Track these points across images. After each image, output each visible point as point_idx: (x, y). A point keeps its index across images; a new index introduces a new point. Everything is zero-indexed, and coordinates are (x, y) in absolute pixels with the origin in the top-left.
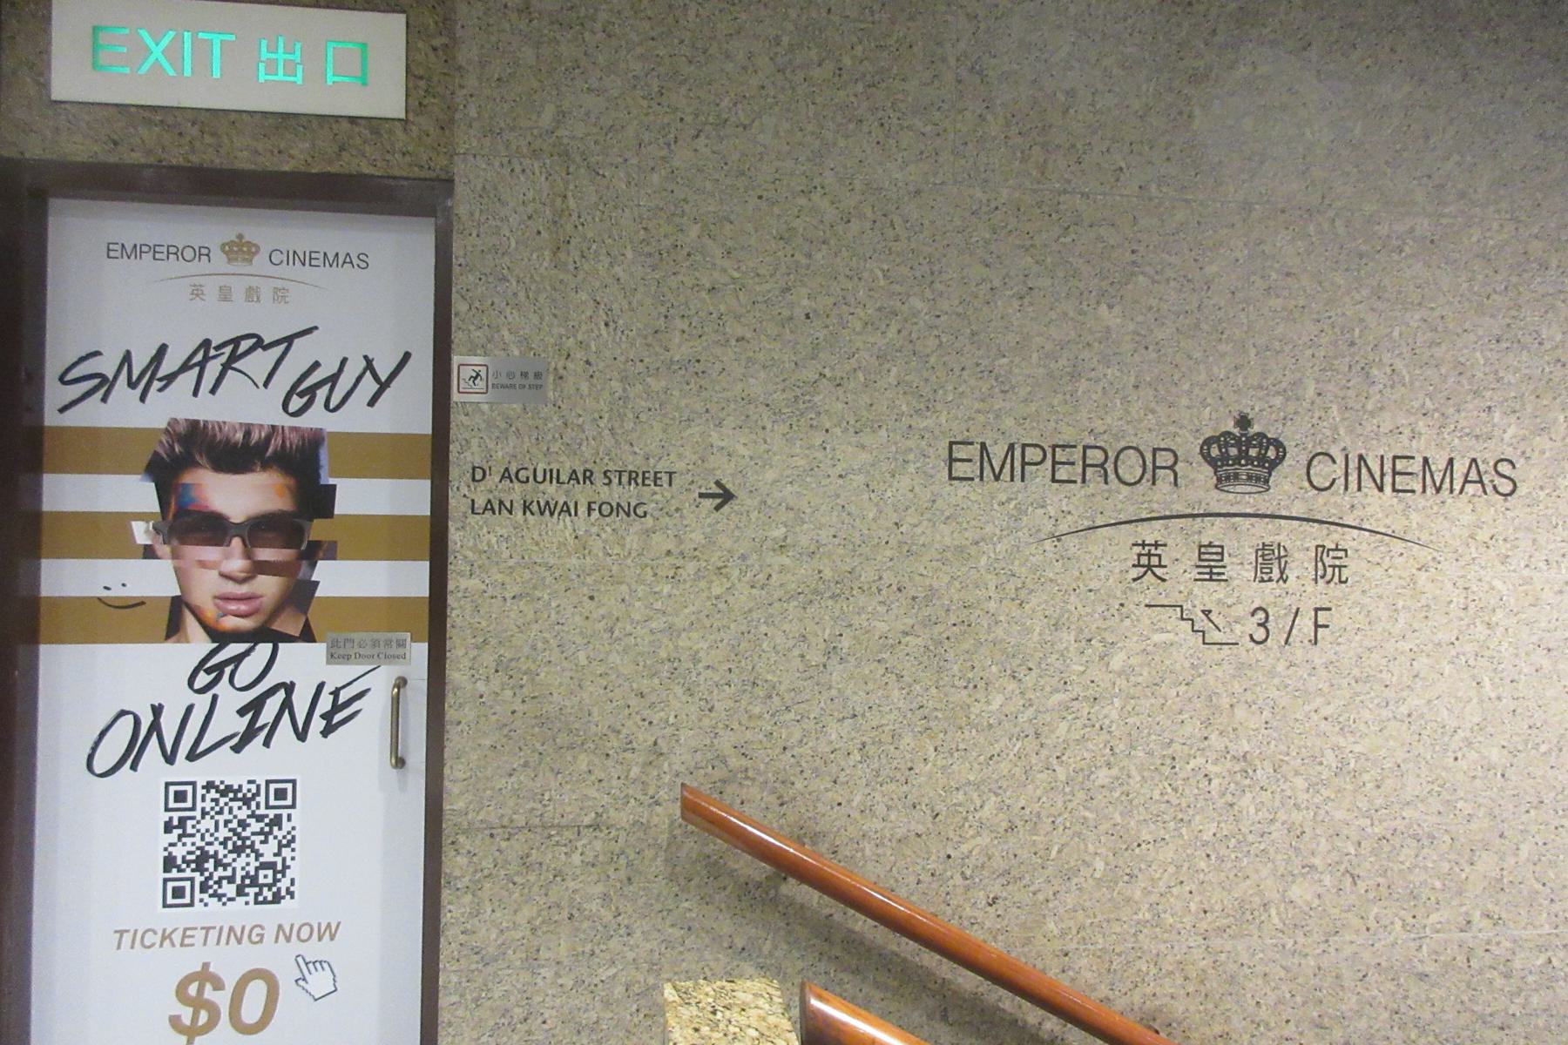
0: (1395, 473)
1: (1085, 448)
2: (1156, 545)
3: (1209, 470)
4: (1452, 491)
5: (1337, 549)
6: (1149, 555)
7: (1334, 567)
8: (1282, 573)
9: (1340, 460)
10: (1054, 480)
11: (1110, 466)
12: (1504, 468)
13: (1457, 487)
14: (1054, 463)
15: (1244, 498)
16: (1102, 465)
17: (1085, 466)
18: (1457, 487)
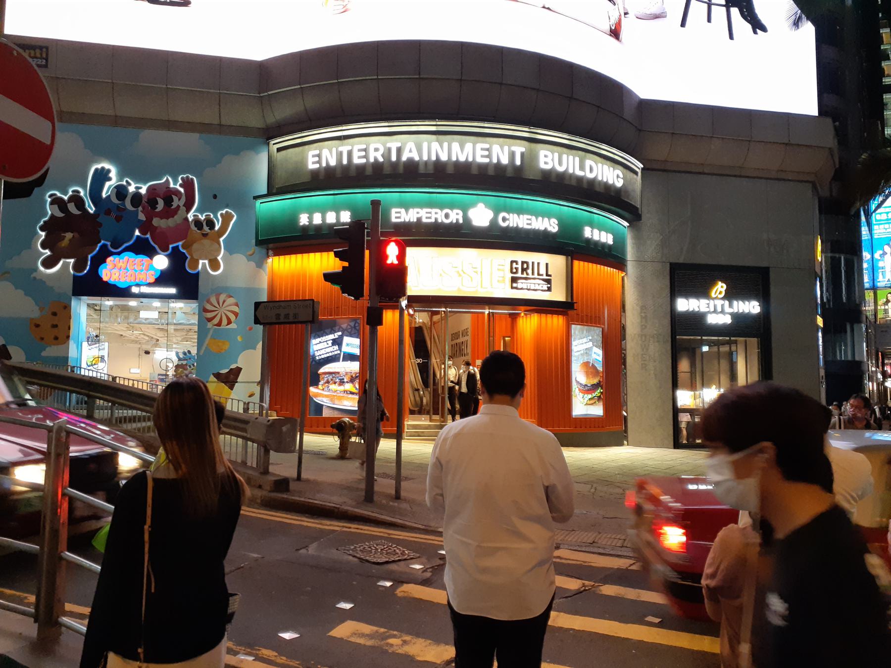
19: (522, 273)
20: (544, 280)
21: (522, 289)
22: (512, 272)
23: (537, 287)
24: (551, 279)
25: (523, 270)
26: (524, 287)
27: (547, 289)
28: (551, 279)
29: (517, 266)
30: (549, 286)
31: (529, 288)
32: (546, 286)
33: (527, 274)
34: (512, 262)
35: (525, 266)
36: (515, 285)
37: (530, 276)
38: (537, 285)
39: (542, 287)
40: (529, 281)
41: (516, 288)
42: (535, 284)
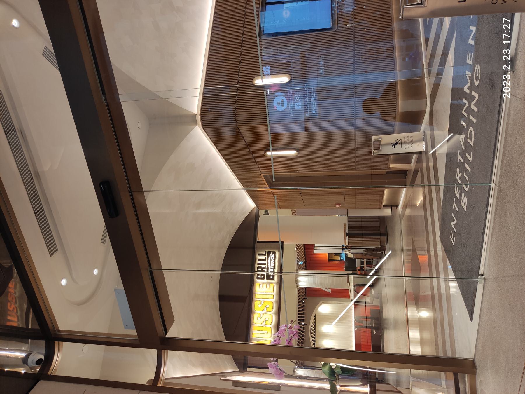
19: (264, 271)
20: (268, 256)
22: (263, 279)
23: (273, 261)
25: (262, 271)
27: (274, 255)
30: (272, 253)
31: (273, 267)
33: (265, 268)
34: (258, 278)
35: (260, 269)
36: (271, 277)
37: (266, 266)
39: (272, 258)
40: (269, 267)
41: (273, 276)
42: (271, 263)
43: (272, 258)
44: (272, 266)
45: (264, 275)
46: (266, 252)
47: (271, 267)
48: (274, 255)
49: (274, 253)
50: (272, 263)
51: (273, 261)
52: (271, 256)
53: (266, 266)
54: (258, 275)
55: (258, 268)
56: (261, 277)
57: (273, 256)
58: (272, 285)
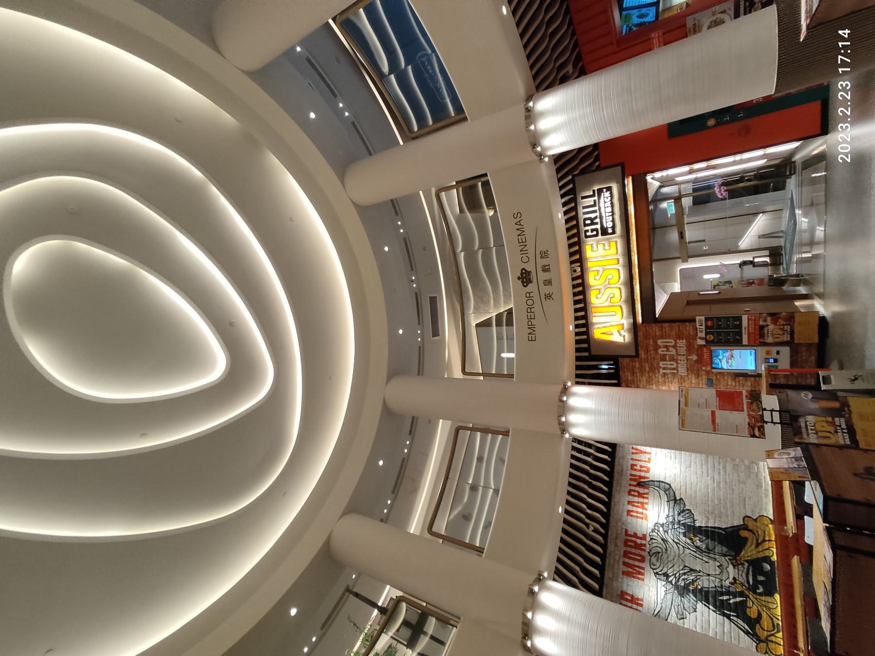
0: (522, 242)
1: (528, 312)
2: (545, 295)
3: (529, 285)
4: (523, 228)
5: (541, 254)
6: (548, 297)
7: (545, 254)
8: (547, 266)
9: (523, 255)
10: (534, 319)
11: (530, 307)
12: (515, 216)
13: (522, 227)
14: (531, 319)
15: (533, 276)
16: (531, 308)
17: (531, 312)
18: (522, 227)
19: (597, 223)
20: (599, 198)
21: (613, 221)
22: (597, 235)
23: (609, 204)
24: (591, 229)
25: (593, 223)
26: (611, 219)
27: (609, 192)
28: (591, 229)
29: (590, 231)
30: (605, 190)
32: (605, 193)
33: (596, 218)
35: (588, 222)
36: (610, 231)
37: (598, 214)
38: (607, 205)
40: (603, 215)
41: (613, 227)
42: (605, 207)
43: (607, 198)
44: (608, 213)
45: (596, 230)
46: (594, 191)
47: (607, 214)
48: (609, 192)
49: (609, 189)
50: (608, 207)
51: (610, 202)
52: (605, 196)
53: (598, 214)
54: (587, 231)
55: (585, 219)
56: (593, 234)
57: (607, 194)
58: (613, 245)
